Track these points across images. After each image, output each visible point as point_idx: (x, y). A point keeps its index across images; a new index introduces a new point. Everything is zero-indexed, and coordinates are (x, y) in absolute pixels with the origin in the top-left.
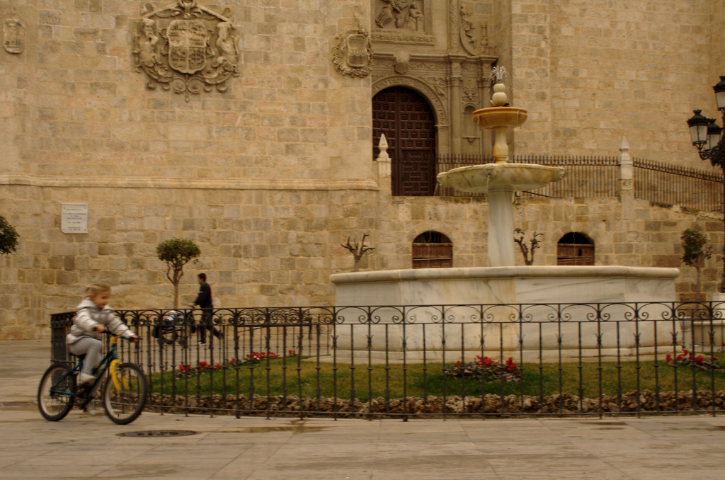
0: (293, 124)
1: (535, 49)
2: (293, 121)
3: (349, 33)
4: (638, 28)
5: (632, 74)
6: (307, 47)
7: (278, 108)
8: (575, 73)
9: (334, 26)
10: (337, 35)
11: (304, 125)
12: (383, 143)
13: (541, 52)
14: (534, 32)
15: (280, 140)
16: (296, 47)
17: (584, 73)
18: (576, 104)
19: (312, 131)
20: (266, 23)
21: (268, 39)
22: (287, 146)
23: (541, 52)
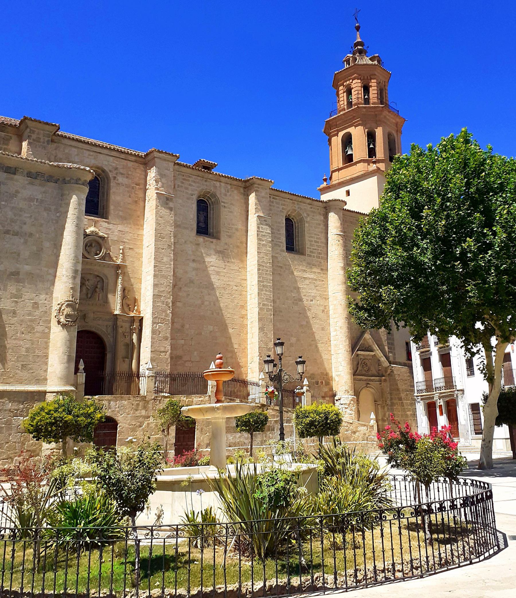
0: (27, 352)
1: (164, 314)
2: (27, 350)
3: (67, 301)
4: (214, 305)
5: (211, 328)
6: (40, 308)
7: (19, 343)
8: (183, 326)
9: (58, 297)
10: (59, 302)
11: (34, 353)
12: (82, 366)
13: (167, 315)
14: (163, 304)
15: (18, 361)
16: (33, 307)
17: (187, 326)
18: (182, 342)
19: (38, 356)
20: (16, 293)
21: (16, 302)
22: (22, 365)
23: (167, 315)
